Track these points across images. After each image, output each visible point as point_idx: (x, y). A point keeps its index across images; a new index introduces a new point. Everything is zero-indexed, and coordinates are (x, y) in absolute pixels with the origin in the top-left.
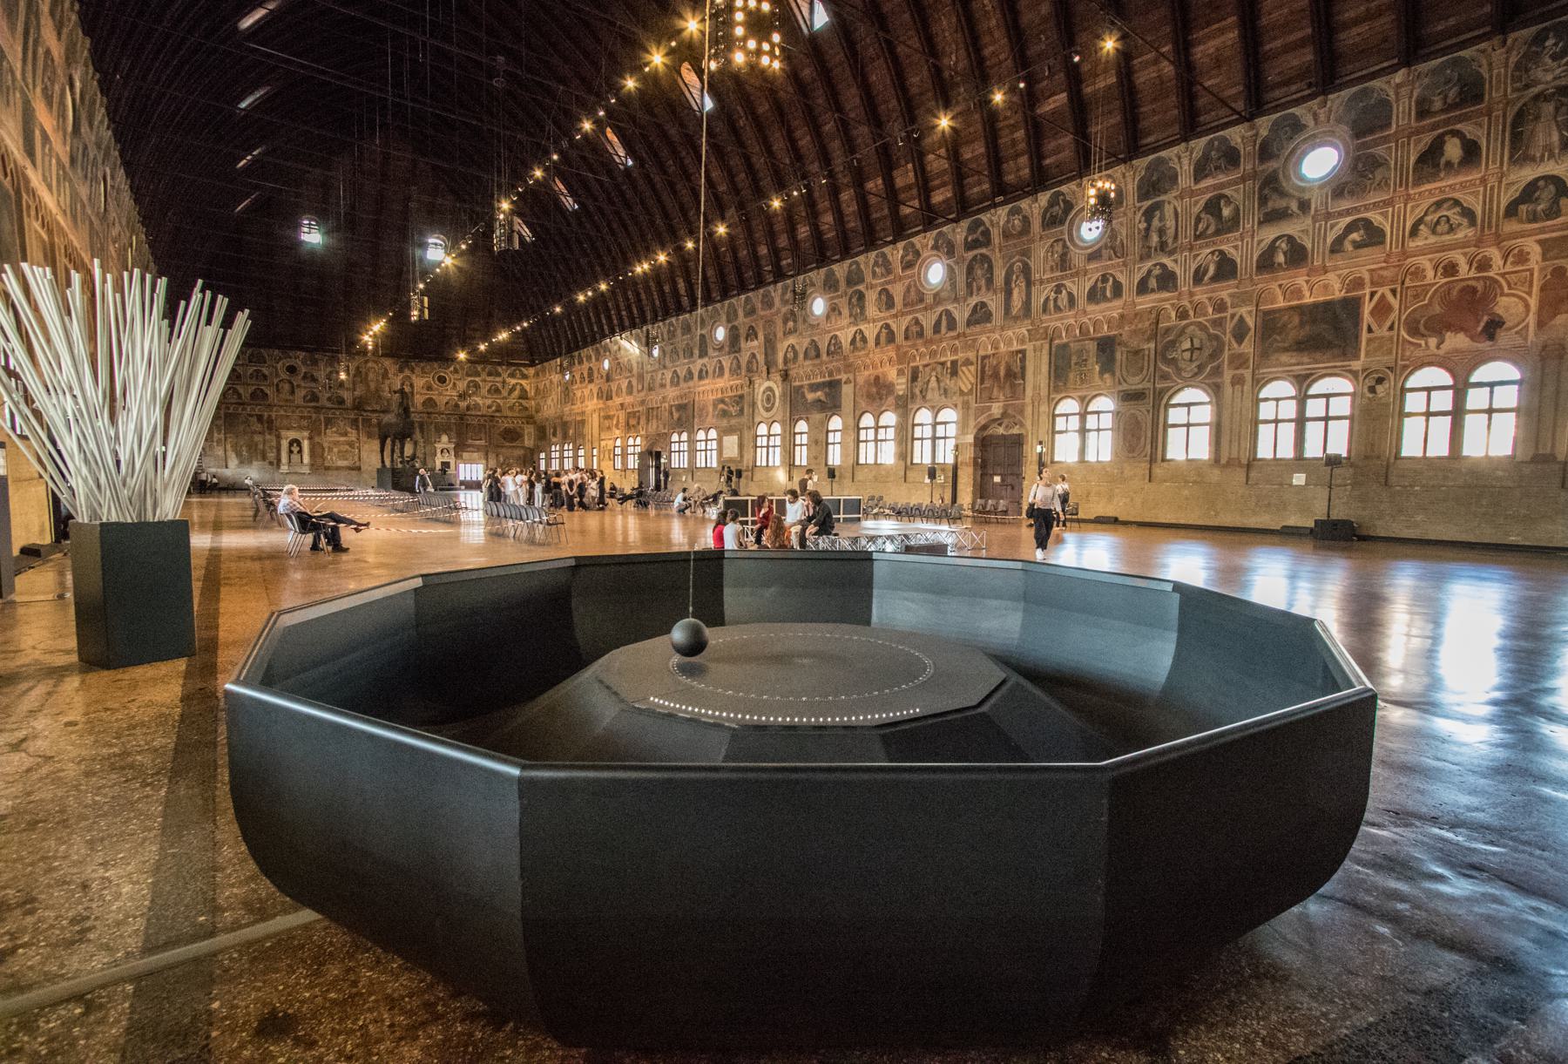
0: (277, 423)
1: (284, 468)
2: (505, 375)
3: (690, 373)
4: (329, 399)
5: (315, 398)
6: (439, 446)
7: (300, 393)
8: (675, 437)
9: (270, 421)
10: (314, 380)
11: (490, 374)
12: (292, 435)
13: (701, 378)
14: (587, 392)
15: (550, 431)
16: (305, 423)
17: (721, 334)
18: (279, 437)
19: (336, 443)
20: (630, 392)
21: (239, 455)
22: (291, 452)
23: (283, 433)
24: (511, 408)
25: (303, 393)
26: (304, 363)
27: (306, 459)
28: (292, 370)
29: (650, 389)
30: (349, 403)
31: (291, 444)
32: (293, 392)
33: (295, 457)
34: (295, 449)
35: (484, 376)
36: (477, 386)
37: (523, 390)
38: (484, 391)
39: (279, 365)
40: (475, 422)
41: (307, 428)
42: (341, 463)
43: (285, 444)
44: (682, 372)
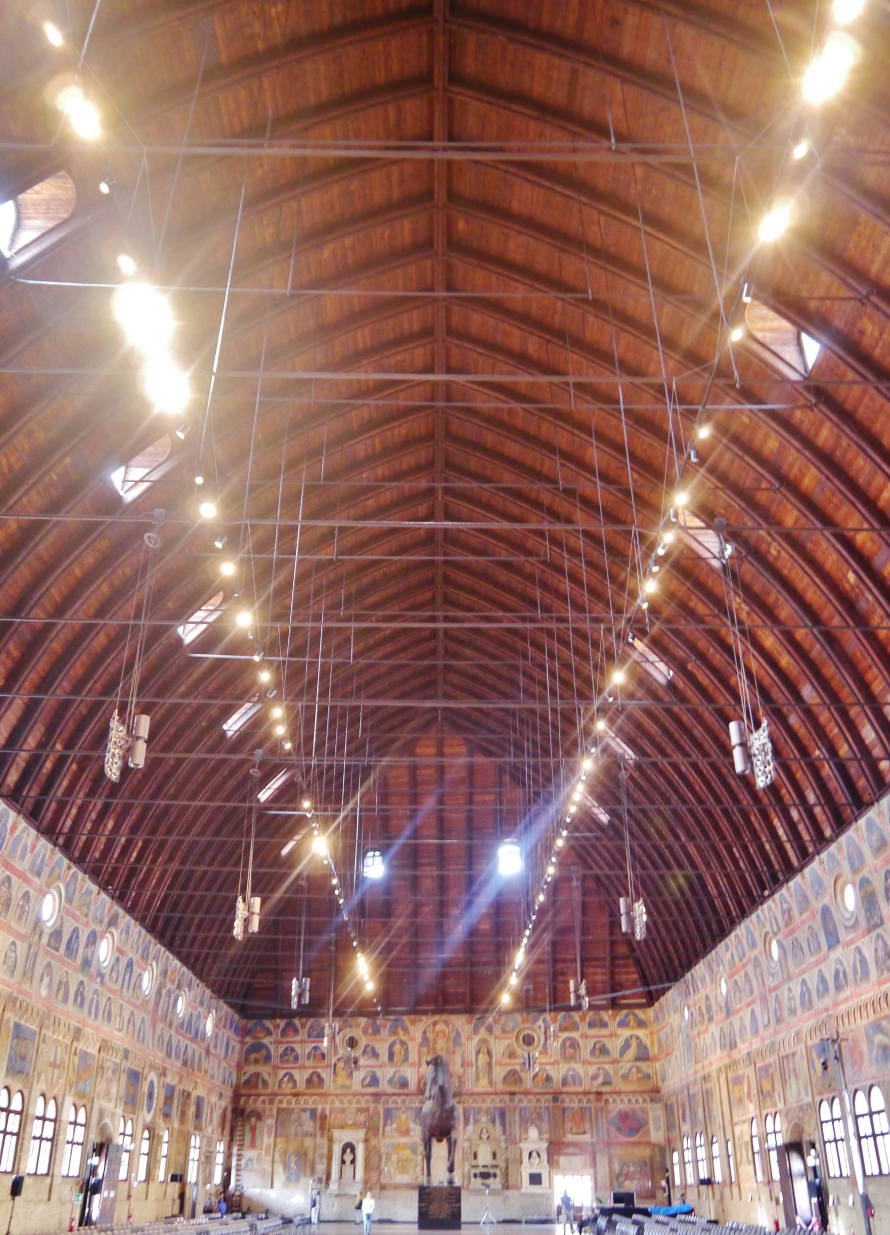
0: (331, 1120)
1: (333, 1186)
2: (613, 1025)
3: (823, 980)
4: (390, 1081)
5: (374, 1081)
6: (526, 1147)
8: (825, 1114)
9: (324, 1118)
10: (375, 1055)
11: (591, 1025)
13: (838, 988)
14: (708, 1037)
15: (678, 1112)
16: (361, 1118)
17: (850, 898)
18: (331, 1140)
19: (396, 1147)
20: (756, 1032)
21: (286, 1166)
22: (343, 1162)
23: (337, 1134)
24: (625, 1077)
26: (365, 1032)
27: (360, 1174)
28: (352, 1043)
29: (779, 1021)
30: (413, 1086)
31: (344, 1151)
32: (350, 1075)
33: (348, 1168)
34: (348, 1157)
35: (584, 1028)
36: (574, 1045)
37: (641, 1046)
38: (585, 1054)
40: (575, 1105)
41: (364, 1125)
44: (813, 982)
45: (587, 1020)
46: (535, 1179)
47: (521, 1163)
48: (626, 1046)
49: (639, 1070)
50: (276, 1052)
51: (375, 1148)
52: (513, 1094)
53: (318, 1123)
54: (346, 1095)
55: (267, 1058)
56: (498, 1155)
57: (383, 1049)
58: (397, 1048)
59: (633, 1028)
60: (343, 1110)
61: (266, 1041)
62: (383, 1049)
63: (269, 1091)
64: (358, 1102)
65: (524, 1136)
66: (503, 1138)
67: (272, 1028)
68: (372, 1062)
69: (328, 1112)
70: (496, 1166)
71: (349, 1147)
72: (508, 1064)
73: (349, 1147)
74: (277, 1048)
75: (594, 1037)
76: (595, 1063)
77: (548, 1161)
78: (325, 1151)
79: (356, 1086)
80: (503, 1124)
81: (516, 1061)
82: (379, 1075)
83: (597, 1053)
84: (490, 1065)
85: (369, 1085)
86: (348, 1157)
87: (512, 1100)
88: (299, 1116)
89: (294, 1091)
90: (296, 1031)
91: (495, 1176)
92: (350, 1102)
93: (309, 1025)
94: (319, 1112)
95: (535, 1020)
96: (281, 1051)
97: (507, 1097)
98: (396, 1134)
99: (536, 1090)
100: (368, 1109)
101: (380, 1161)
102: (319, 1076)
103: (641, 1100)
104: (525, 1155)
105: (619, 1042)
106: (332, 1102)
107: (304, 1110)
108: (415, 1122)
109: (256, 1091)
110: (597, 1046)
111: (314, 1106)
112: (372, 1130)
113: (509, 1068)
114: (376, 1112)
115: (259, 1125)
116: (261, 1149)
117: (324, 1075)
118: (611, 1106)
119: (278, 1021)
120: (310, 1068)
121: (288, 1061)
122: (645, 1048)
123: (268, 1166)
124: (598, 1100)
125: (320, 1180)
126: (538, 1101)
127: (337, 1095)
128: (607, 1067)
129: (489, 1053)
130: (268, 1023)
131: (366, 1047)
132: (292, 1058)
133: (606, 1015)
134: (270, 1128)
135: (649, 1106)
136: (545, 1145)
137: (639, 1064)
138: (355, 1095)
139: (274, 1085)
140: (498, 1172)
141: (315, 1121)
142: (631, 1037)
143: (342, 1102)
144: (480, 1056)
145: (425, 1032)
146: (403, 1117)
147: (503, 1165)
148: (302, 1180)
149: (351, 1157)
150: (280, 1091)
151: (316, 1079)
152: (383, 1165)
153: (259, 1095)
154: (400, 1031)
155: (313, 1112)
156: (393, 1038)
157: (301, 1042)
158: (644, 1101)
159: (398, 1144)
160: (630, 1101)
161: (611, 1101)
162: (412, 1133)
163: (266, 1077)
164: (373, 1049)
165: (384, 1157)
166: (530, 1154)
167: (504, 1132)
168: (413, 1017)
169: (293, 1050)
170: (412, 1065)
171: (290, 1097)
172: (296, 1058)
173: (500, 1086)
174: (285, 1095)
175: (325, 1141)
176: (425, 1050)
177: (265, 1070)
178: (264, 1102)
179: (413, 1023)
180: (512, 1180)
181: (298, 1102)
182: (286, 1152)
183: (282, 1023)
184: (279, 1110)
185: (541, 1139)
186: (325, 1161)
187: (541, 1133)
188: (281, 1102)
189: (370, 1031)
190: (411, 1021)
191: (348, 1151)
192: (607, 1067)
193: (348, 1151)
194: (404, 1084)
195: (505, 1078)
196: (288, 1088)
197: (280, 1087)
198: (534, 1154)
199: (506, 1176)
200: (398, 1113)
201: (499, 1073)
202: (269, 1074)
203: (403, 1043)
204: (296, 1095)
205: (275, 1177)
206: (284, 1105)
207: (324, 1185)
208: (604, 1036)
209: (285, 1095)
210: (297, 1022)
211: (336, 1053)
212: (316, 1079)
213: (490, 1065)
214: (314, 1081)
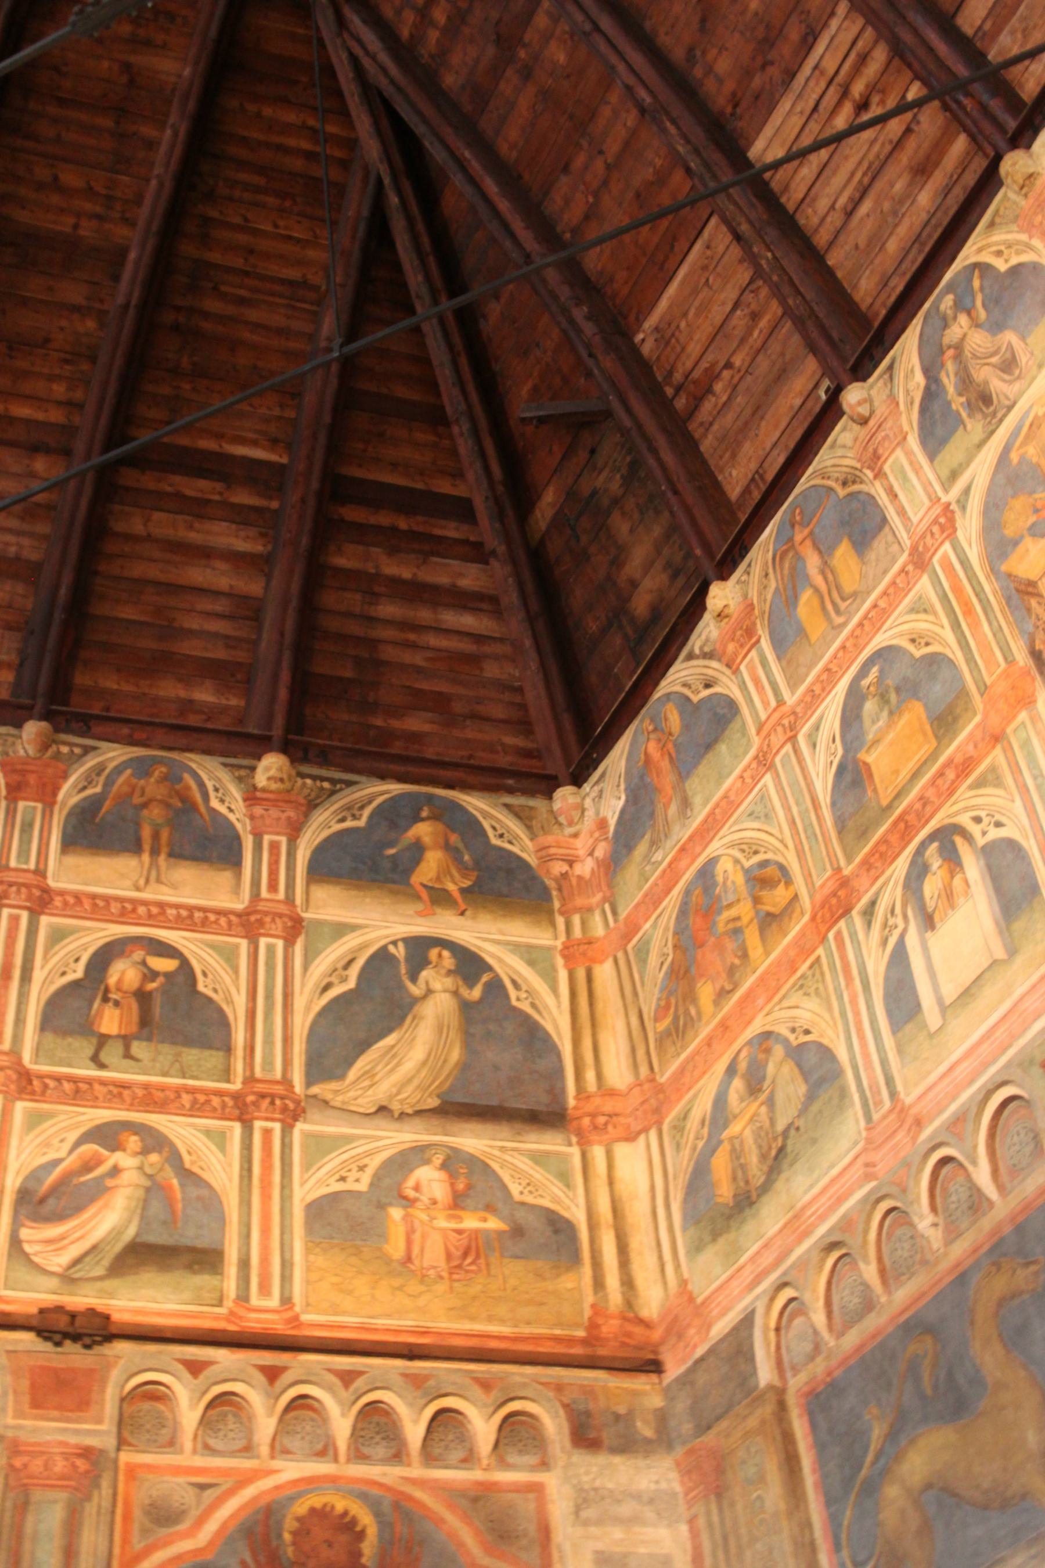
45: (69, 793)
48: (376, 1001)
49: (471, 1182)
59: (439, 898)
75: (99, 907)
76: (80, 1092)
83: (110, 1021)
103: (483, 1427)
105: (317, 977)
110: (124, 973)
118: (177, 1462)
122: (533, 1036)
124: (56, 1392)
128: (181, 1130)
133: (221, 789)
135: (562, 1481)
137: (473, 1140)
142: (420, 949)
158: (516, 1431)
160: (375, 1423)
161: (188, 1408)
192: (181, 1130)
208: (192, 919)
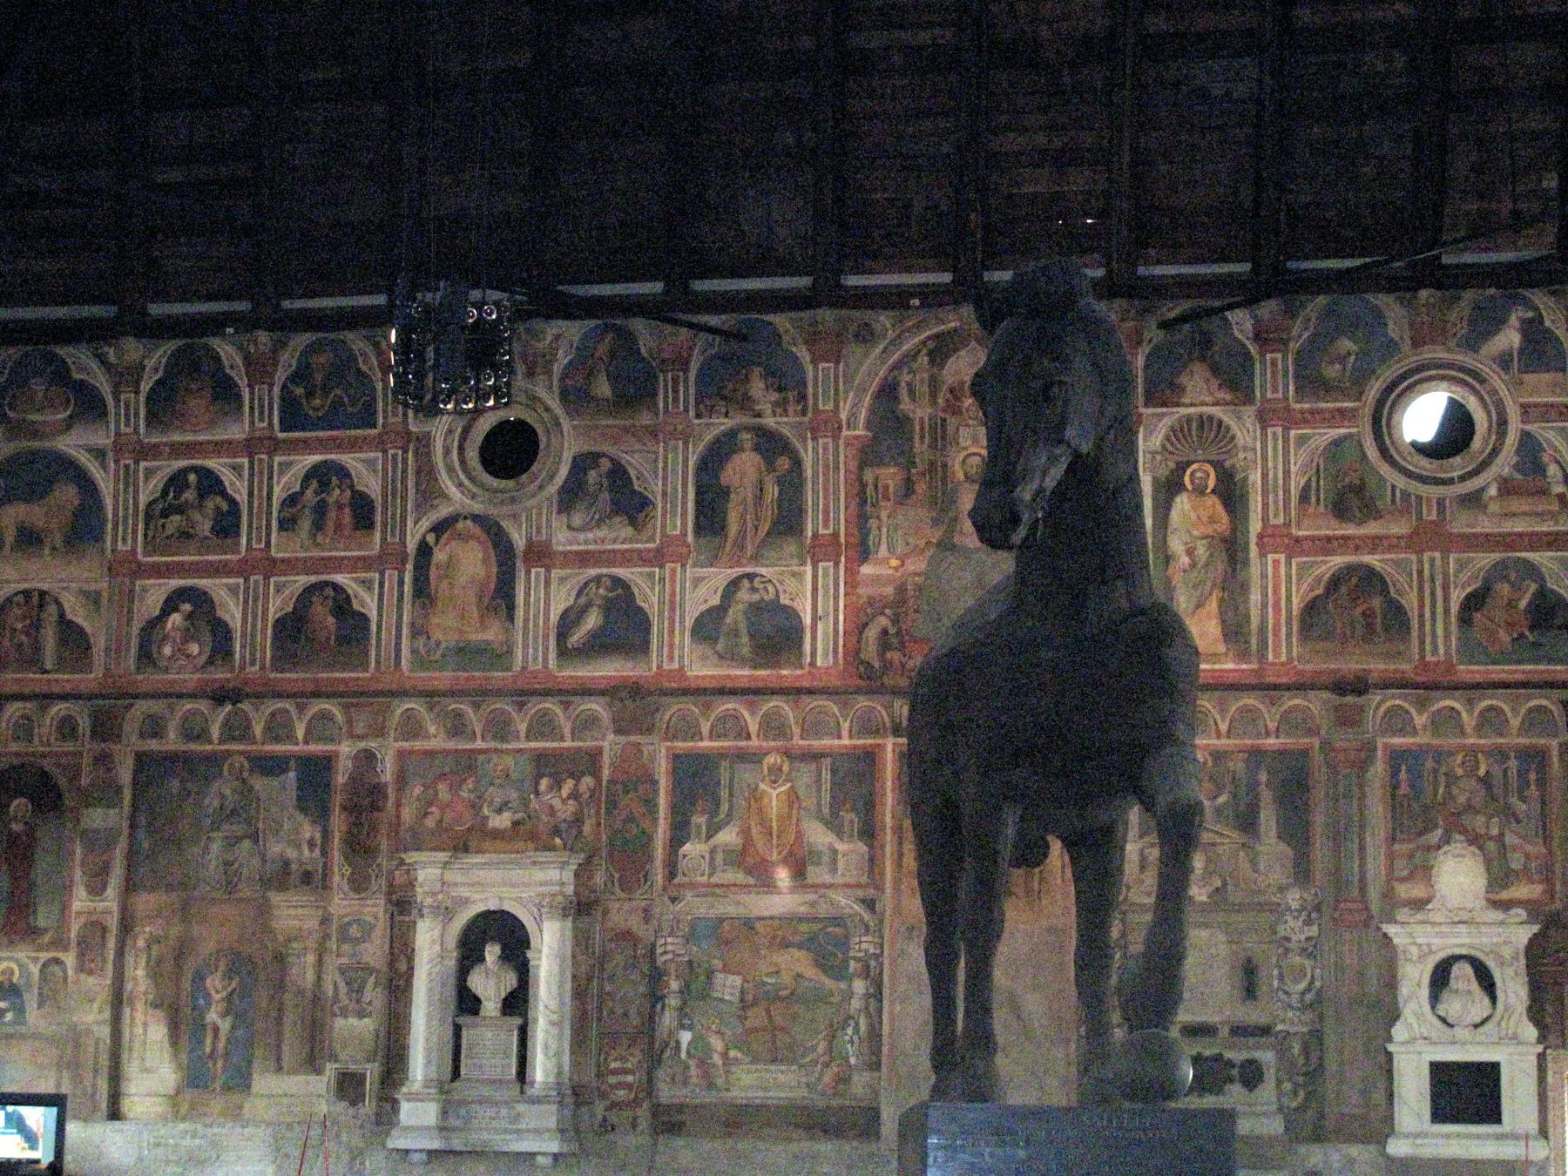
1: (418, 1115)
4: (707, 628)
5: (625, 626)
6: (1418, 942)
7: (546, 597)
9: (367, 799)
10: (630, 503)
12: (492, 884)
16: (558, 801)
18: (402, 905)
21: (183, 1025)
22: (468, 1003)
23: (428, 871)
25: (561, 601)
26: (576, 397)
30: (823, 647)
32: (501, 598)
33: (489, 1040)
34: (490, 983)
39: (440, 429)
42: (750, 1082)
43: (432, 945)
46: (1467, 1093)
47: (1394, 1016)
50: (126, 492)
51: (627, 936)
52: (1359, 686)
53: (338, 823)
54: (479, 695)
55: (84, 527)
56: (1269, 978)
57: (668, 476)
58: (743, 468)
60: (467, 764)
61: (74, 444)
62: (668, 476)
63: (90, 679)
64: (543, 726)
65: (1403, 891)
66: (1294, 898)
67: (102, 383)
68: (616, 535)
69: (387, 772)
70: (1265, 1031)
71: (500, 934)
72: (1327, 545)
73: (500, 934)
74: (128, 480)
77: (1536, 1013)
78: (374, 952)
79: (532, 650)
80: (1296, 831)
81: (1372, 528)
82: (649, 598)
84: (1232, 548)
85: (600, 645)
86: (490, 983)
87: (1348, 719)
88: (246, 791)
89: (220, 674)
90: (225, 393)
91: (1251, 1076)
92: (500, 728)
93: (288, 360)
94: (341, 779)
95: (1485, 324)
96: (148, 491)
97: (1317, 704)
98: (740, 877)
99: (1469, 671)
100: (593, 759)
101: (656, 998)
102: (342, 606)
104: (1414, 979)
106: (412, 728)
107: (271, 766)
108: (833, 824)
109: (33, 680)
111: (315, 748)
112: (615, 857)
113: (1338, 561)
114: (637, 780)
115: (46, 837)
116: (60, 943)
117: (367, 603)
119: (132, 349)
120: (290, 566)
121: (185, 535)
123: (93, 1018)
125: (348, 1087)
126: (1491, 721)
127: (429, 695)
129: (1231, 493)
130: (81, 360)
131: (582, 464)
132: (205, 526)
134: (98, 843)
136: (1523, 935)
138: (522, 695)
139: (116, 648)
140: (1267, 1057)
141: (321, 815)
143: (458, 728)
144: (1182, 503)
145: (888, 391)
146: (774, 796)
147: (1292, 1022)
148: (265, 1083)
149: (510, 980)
150: (150, 679)
151: (324, 618)
152: (667, 1019)
153: (46, 698)
154: (757, 387)
155: (314, 775)
156: (722, 424)
157: (250, 447)
159: (749, 924)
162: (815, 874)
163: (78, 614)
164: (618, 474)
165: (674, 985)
166: (1440, 978)
167: (1302, 872)
168: (827, 315)
169: (210, 484)
170: (822, 549)
171: (203, 706)
172: (227, 526)
173: (1285, 652)
174: (172, 695)
175: (375, 909)
176: (890, 476)
177: (69, 581)
178: (67, 728)
179: (828, 347)
180: (1343, 1095)
181: (237, 730)
182: (180, 953)
183: (155, 358)
184: (143, 760)
185: (1505, 906)
186: (374, 995)
187: (1499, 877)
188: (154, 728)
189: (603, 388)
190: (812, 340)
191: (492, 952)
193: (492, 952)
194: (777, 635)
195: (1311, 609)
196: (184, 662)
197: (146, 656)
198: (1462, 974)
199: (1310, 1074)
200: (746, 775)
201: (1280, 585)
202: (94, 599)
203: (771, 445)
204: (220, 696)
205: (131, 1069)
206: (172, 741)
207: (368, 1107)
209: (172, 695)
210: (226, 350)
211: (429, 493)
212: (324, 618)
213: (1232, 548)
214: (321, 631)
